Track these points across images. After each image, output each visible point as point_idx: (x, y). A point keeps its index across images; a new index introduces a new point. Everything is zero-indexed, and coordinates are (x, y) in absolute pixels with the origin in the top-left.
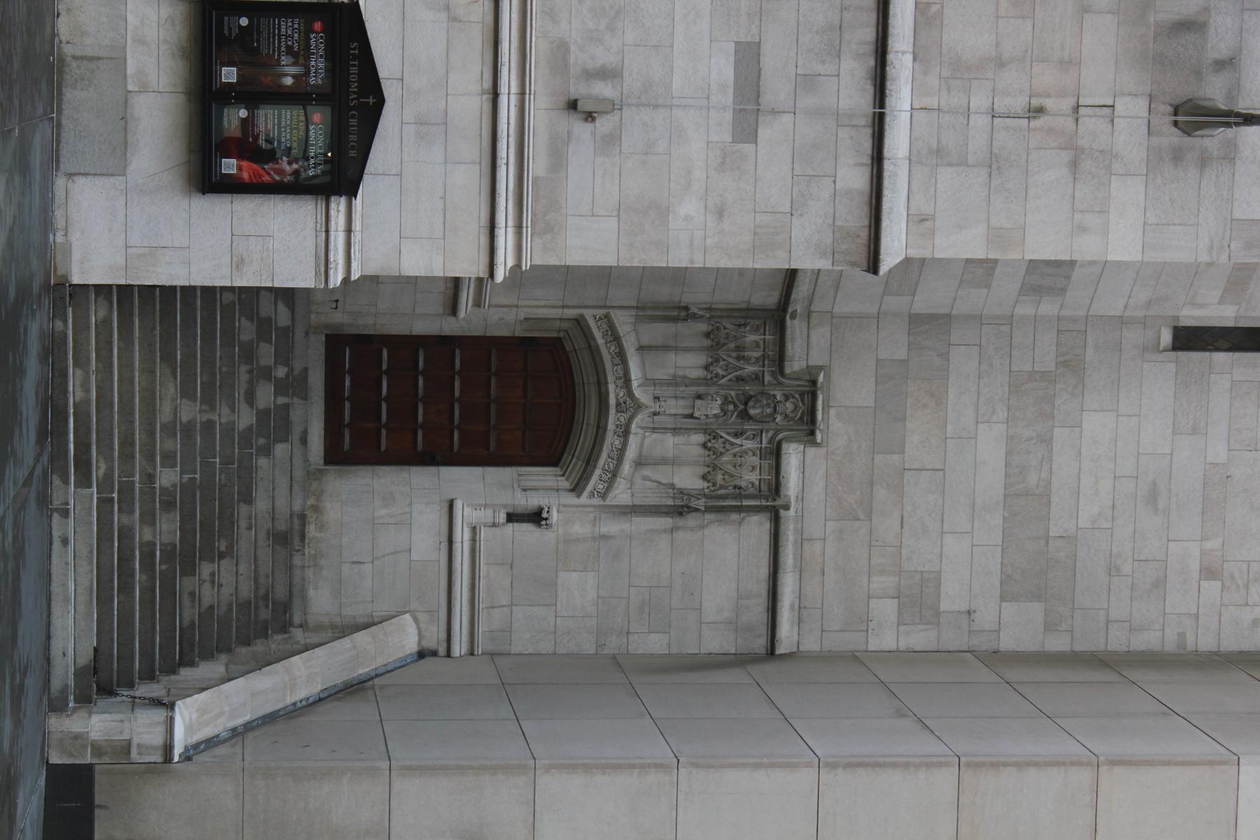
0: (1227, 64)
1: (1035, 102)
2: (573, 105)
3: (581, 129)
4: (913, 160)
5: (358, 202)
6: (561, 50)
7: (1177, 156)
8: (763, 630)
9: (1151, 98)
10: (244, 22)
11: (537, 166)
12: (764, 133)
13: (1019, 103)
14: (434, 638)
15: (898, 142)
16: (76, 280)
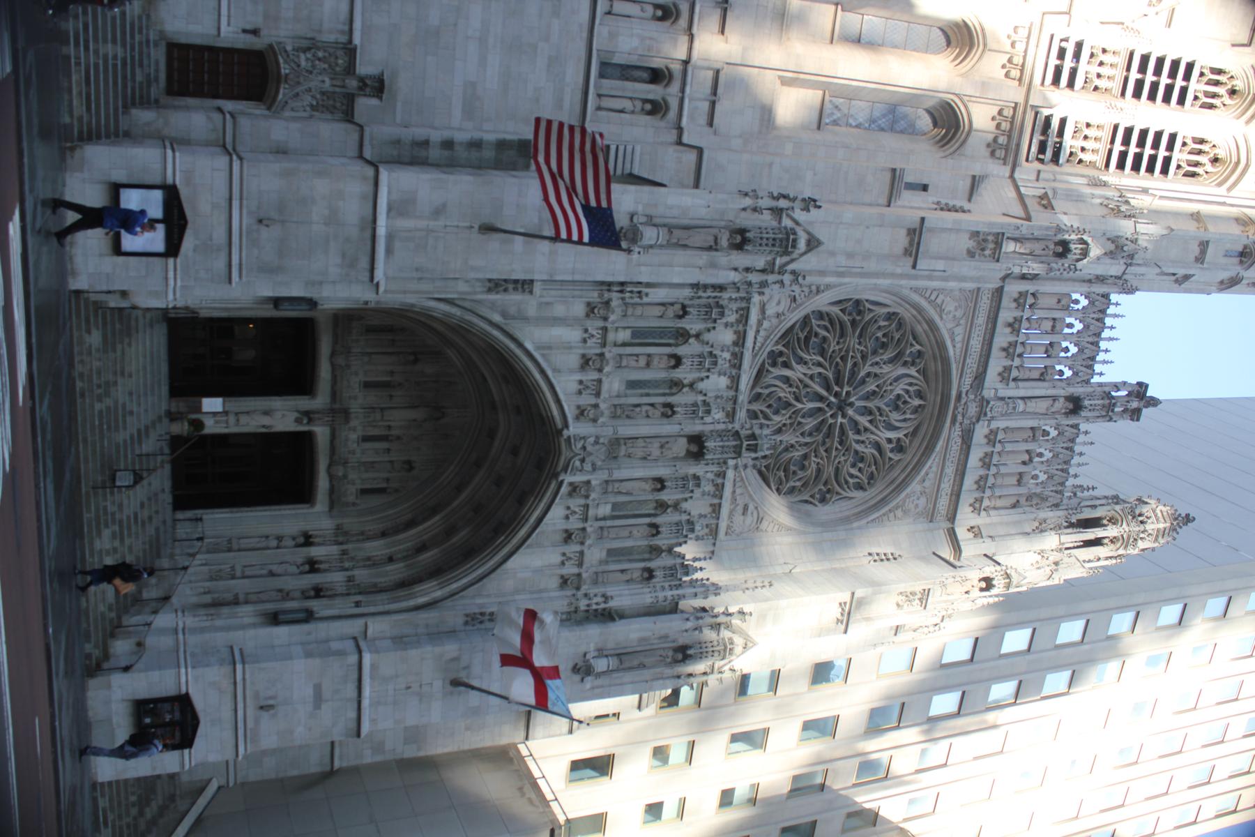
0: (467, 667)
1: (409, 685)
2: (262, 708)
3: (265, 714)
4: (370, 705)
5: (193, 750)
6: (257, 695)
7: (452, 693)
8: (329, 764)
9: (444, 680)
10: (153, 730)
11: (250, 724)
12: (324, 706)
13: (403, 686)
14: (223, 782)
15: (366, 703)
16: (100, 780)
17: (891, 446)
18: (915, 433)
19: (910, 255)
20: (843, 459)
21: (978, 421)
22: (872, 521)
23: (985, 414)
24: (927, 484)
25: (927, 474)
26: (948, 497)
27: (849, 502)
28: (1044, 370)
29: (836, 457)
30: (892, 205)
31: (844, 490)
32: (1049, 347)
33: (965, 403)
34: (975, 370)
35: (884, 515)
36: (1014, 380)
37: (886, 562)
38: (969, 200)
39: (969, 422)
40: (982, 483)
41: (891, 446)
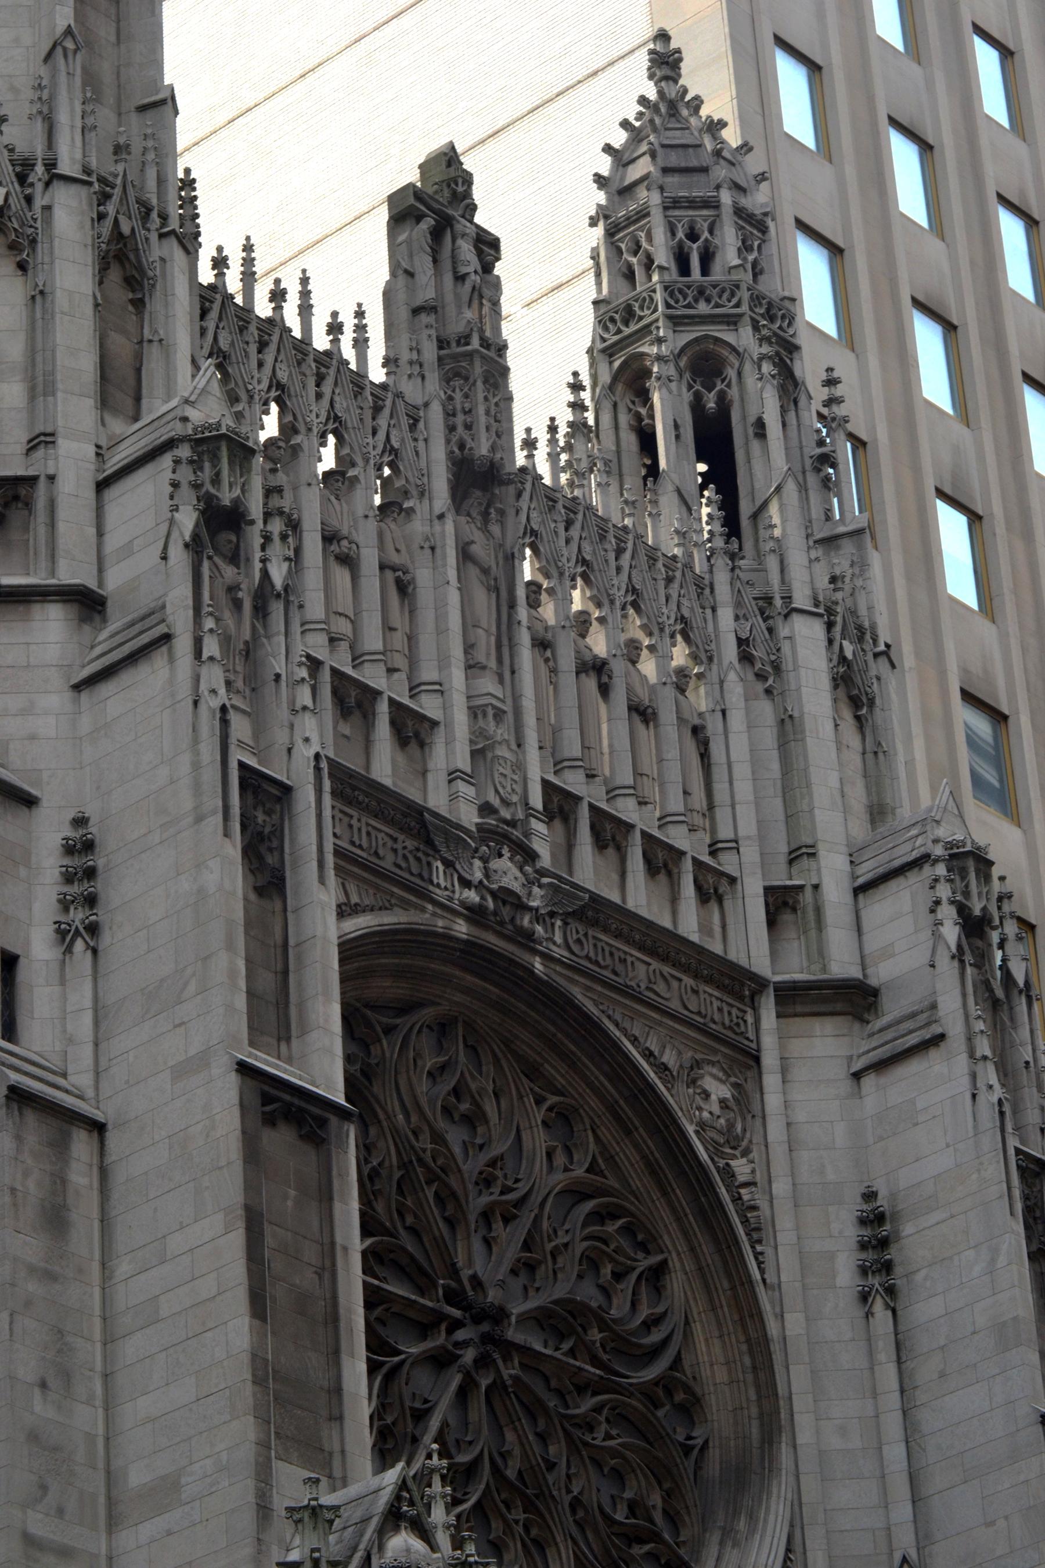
17: (560, 1159)
18: (532, 1072)
19: (323, 1123)
20: (595, 1335)
21: (531, 856)
22: (760, 1264)
23: (512, 823)
24: (669, 1058)
25: (649, 1055)
26: (703, 987)
27: (697, 1329)
28: (390, 576)
29: (595, 1361)
30: (100, 1117)
31: (665, 1342)
32: (334, 547)
33: (494, 894)
34: (410, 844)
35: (745, 1221)
36: (414, 691)
37: (893, 1253)
38: (29, 801)
39: (536, 890)
40: (661, 855)
41: (560, 1159)
